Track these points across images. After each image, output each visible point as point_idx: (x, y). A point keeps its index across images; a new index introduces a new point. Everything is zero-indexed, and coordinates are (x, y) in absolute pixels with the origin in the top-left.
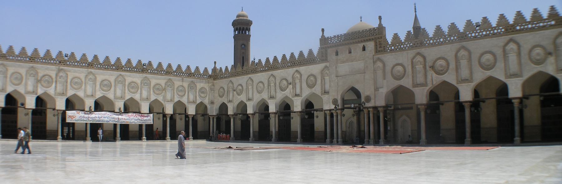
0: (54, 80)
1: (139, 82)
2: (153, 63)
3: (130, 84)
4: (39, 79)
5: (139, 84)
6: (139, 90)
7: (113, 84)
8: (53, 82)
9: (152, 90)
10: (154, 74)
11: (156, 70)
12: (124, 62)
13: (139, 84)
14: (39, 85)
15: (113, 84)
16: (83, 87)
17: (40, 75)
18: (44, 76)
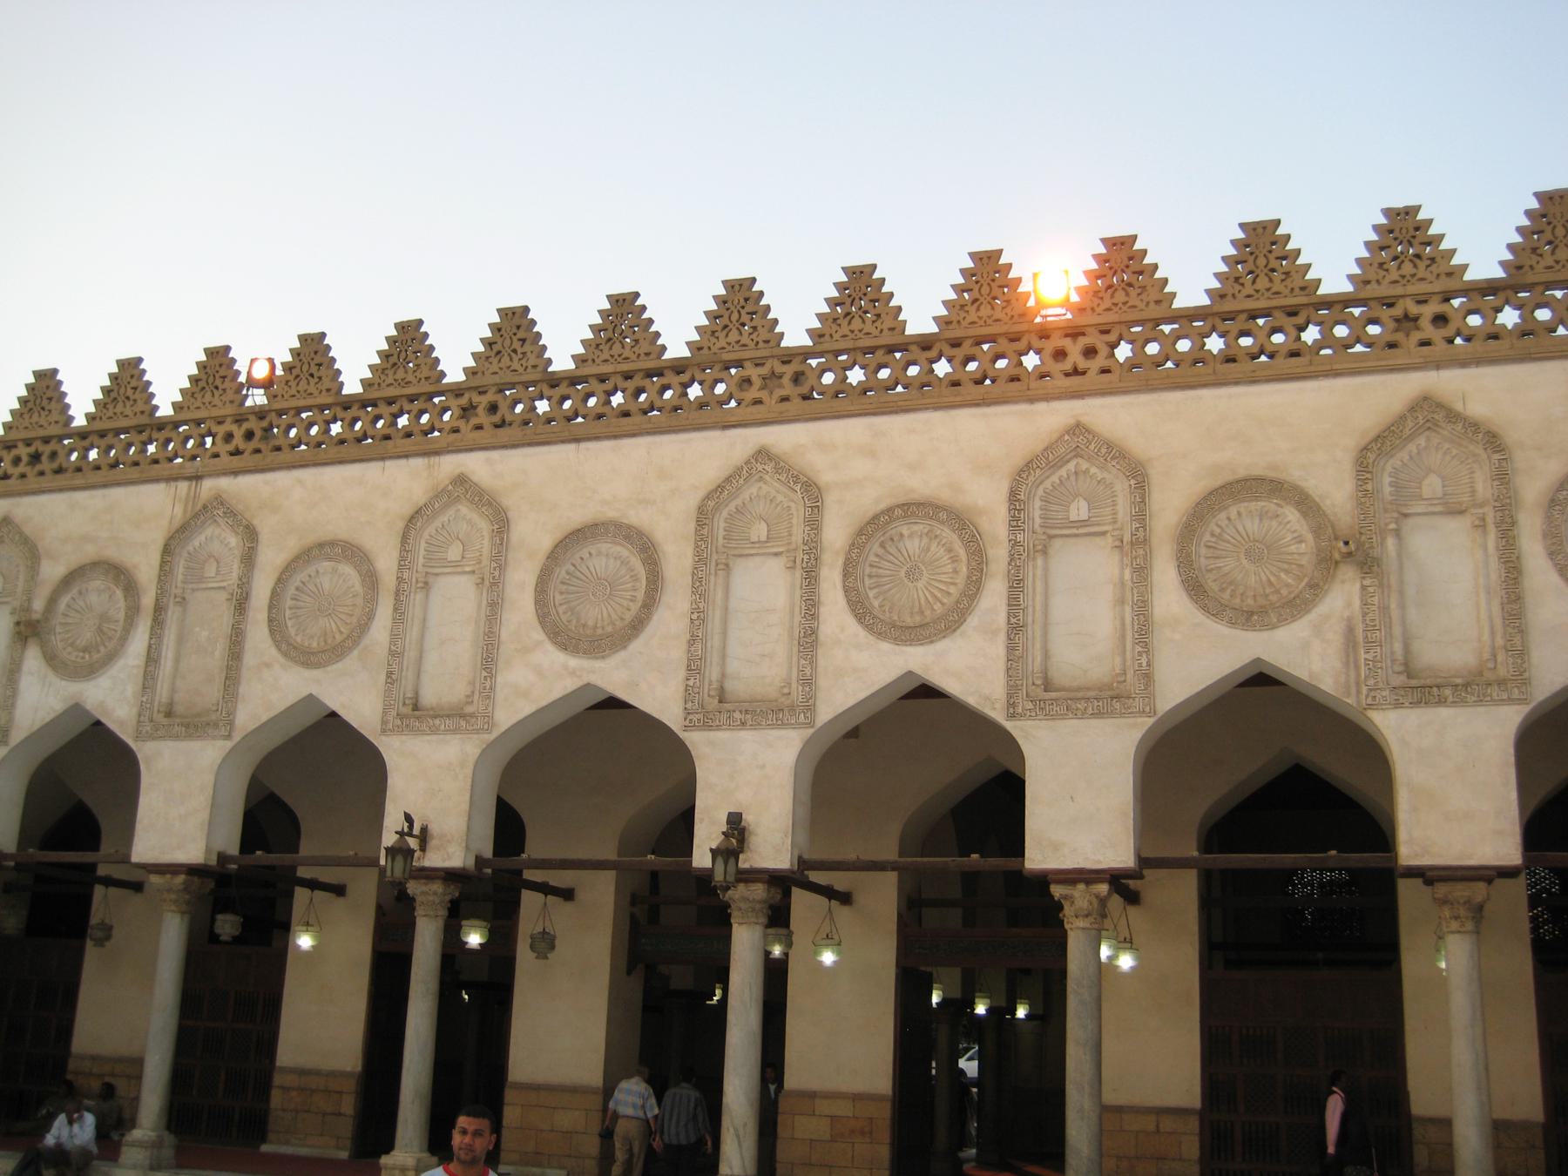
0: (148, 600)
1: (987, 496)
2: (1158, 251)
3: (875, 528)
4: (38, 605)
5: (996, 525)
6: (994, 596)
7: (677, 559)
8: (133, 611)
9: (1166, 575)
10: (1198, 372)
11: (1220, 313)
12: (796, 317)
13: (996, 525)
14: (33, 659)
15: (677, 559)
16: (380, 631)
17: (52, 571)
18: (68, 581)
